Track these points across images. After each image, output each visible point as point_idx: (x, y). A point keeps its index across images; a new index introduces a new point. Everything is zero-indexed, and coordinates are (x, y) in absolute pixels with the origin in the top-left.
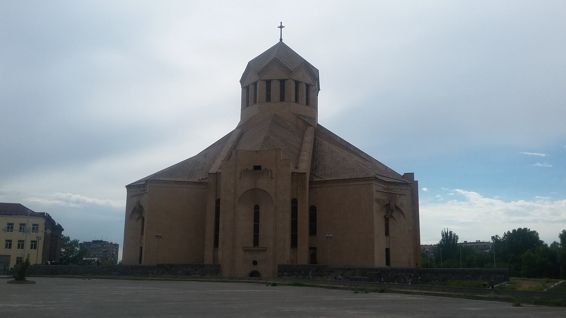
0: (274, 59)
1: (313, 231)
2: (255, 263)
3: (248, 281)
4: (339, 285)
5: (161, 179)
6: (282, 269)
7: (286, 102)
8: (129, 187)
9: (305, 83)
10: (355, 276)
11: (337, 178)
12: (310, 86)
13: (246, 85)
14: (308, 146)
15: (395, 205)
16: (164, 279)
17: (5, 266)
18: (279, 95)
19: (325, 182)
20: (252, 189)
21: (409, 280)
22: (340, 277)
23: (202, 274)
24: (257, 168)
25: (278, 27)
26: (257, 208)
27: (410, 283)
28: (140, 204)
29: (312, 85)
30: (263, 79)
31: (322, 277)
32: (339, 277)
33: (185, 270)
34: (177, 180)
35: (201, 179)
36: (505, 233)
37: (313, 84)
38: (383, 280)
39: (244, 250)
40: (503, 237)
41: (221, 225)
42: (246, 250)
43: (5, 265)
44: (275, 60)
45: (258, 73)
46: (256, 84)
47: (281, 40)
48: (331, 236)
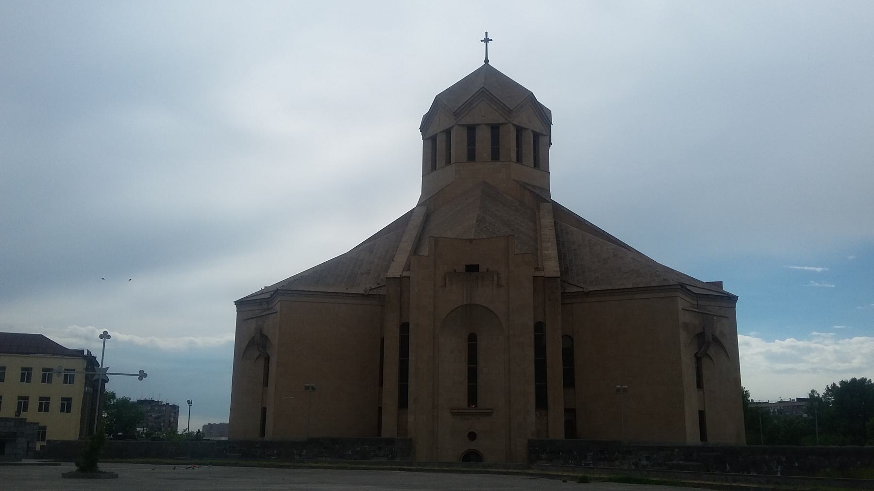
0: (482, 90)
1: (569, 380)
2: (472, 436)
3: (504, 470)
4: (735, 482)
5: (301, 288)
6: (537, 448)
7: (502, 161)
8: (240, 304)
9: (532, 131)
11: (610, 288)
13: (431, 132)
14: (548, 234)
15: (713, 335)
16: (335, 465)
17: (28, 442)
18: (490, 151)
19: (588, 294)
21: (778, 468)
22: (645, 462)
23: (390, 456)
24: (472, 269)
26: (472, 338)
27: (779, 473)
29: (542, 135)
30: (463, 123)
32: (643, 462)
33: (359, 449)
34: (328, 291)
36: (827, 386)
37: (545, 133)
38: (728, 468)
39: (452, 413)
40: (824, 393)
41: (411, 370)
42: (456, 413)
43: (29, 440)
44: (483, 91)
45: (454, 113)
47: (487, 61)
48: (625, 389)
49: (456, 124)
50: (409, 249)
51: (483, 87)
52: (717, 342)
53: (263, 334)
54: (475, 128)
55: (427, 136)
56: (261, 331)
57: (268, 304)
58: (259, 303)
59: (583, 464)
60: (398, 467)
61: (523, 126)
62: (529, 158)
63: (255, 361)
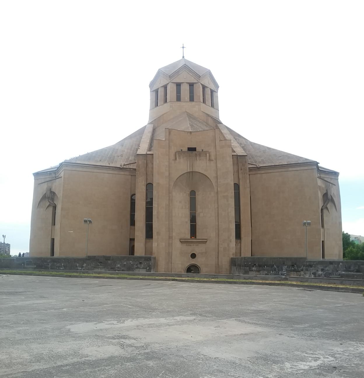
2: (193, 256)
6: (250, 263)
7: (196, 102)
10: (338, 271)
12: (214, 93)
16: (117, 276)
20: (189, 172)
22: (320, 272)
29: (216, 92)
30: (174, 82)
31: (298, 273)
32: (319, 272)
33: (125, 263)
35: (123, 164)
37: (217, 91)
41: (155, 213)
42: (183, 241)
46: (166, 88)
50: (148, 141)
52: (332, 201)
54: (180, 86)
55: (152, 90)
59: (280, 274)
60: (171, 278)
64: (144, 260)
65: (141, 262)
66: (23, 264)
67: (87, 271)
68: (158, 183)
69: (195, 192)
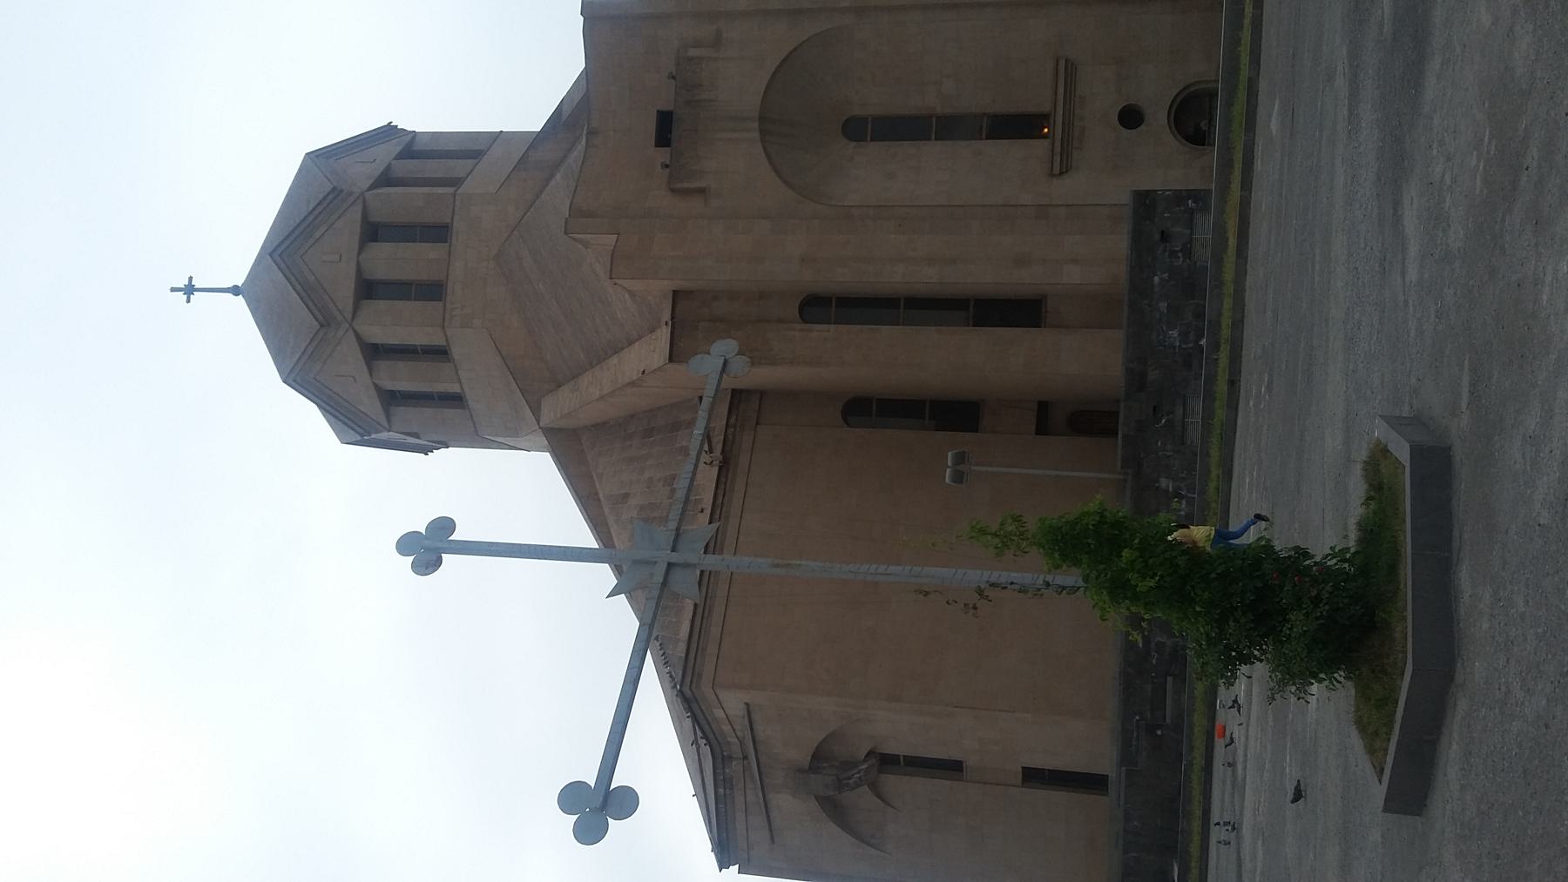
13: (371, 405)
20: (764, 133)
25: (188, 301)
28: (806, 764)
33: (1163, 305)
37: (408, 138)
39: (1061, 173)
44: (280, 255)
45: (322, 326)
47: (235, 290)
49: (351, 325)
51: (271, 255)
53: (810, 768)
55: (383, 420)
56: (801, 771)
57: (731, 758)
58: (725, 789)
61: (382, 169)
62: (458, 167)
63: (889, 804)
64: (1148, 222)
65: (1157, 237)
66: (1159, 732)
67: (1209, 322)
68: (803, 260)
69: (847, 120)
